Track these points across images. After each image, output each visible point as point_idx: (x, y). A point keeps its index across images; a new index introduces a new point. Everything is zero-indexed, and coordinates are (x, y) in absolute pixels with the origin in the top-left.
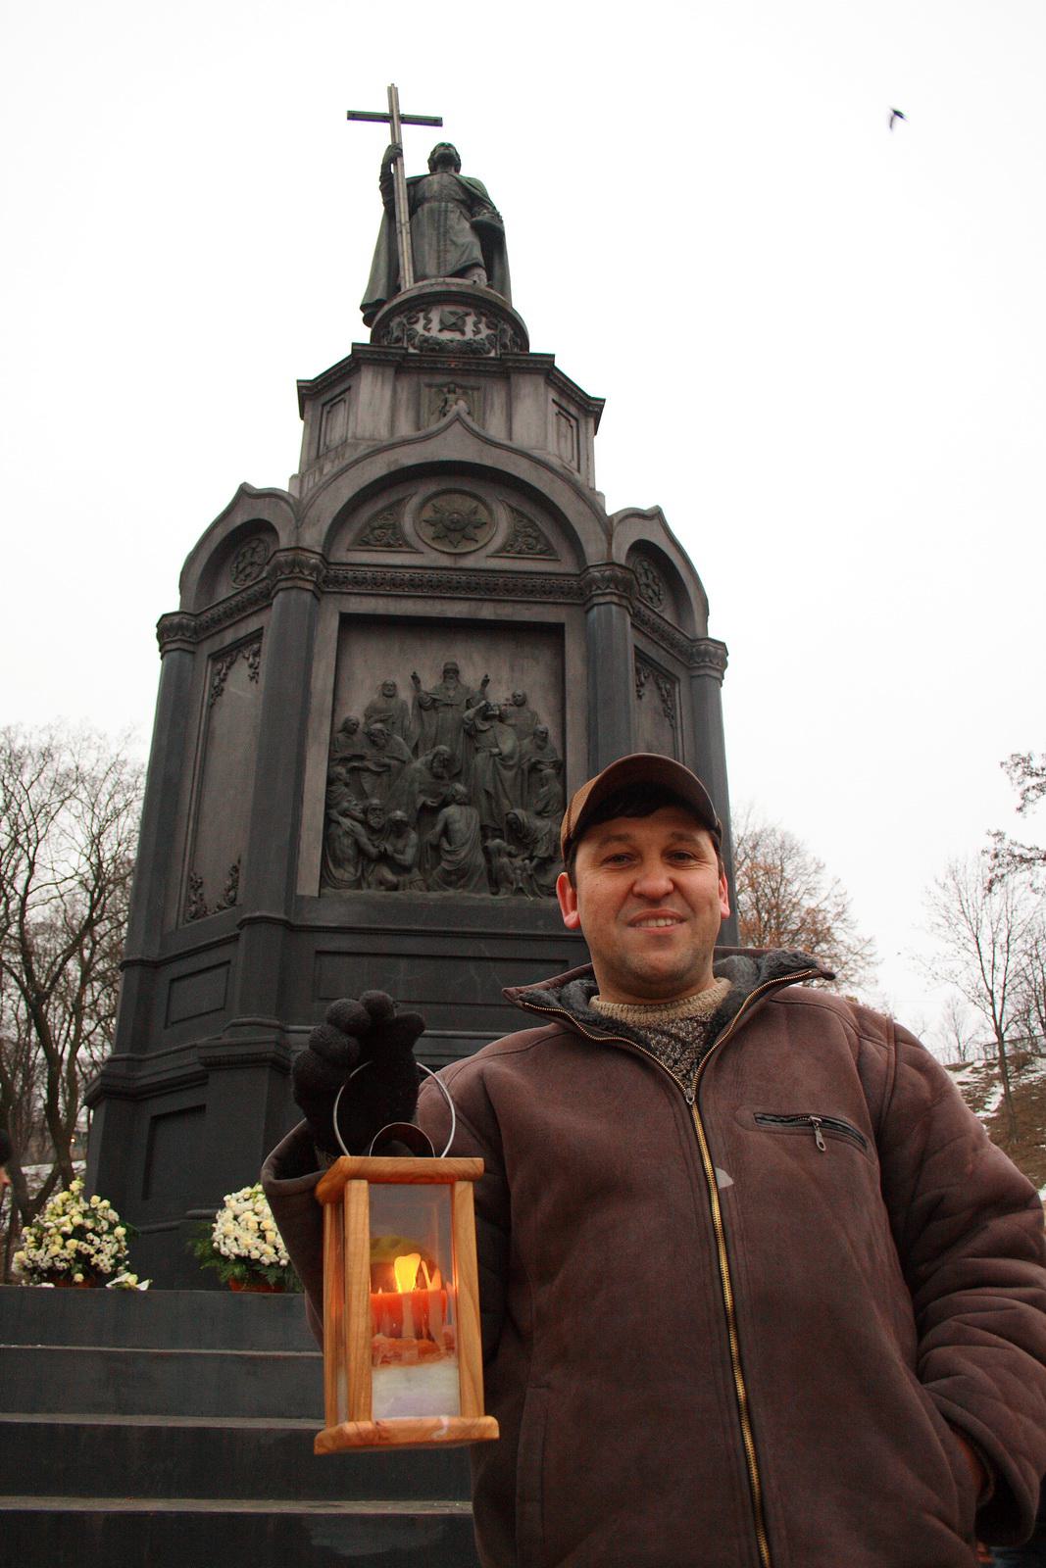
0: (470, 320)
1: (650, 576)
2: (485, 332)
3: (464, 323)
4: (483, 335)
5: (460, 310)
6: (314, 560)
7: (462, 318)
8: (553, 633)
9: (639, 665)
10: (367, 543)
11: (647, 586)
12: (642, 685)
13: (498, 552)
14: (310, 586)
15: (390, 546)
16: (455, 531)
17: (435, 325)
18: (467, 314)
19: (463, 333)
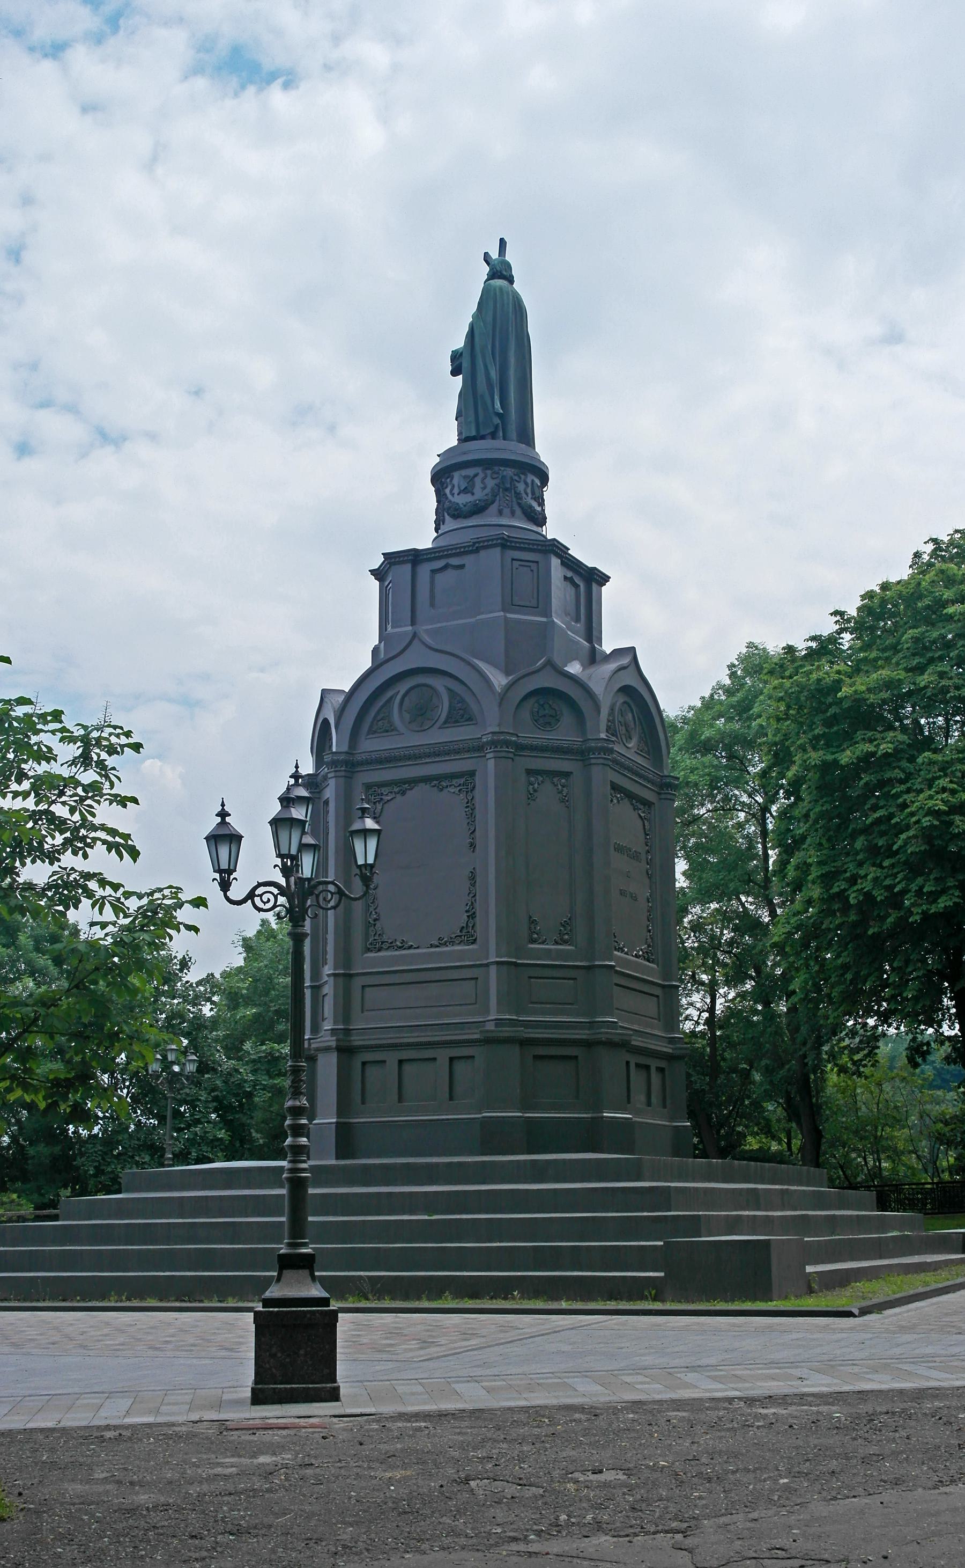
0: (478, 480)
1: (546, 706)
2: (491, 483)
3: (473, 486)
4: (488, 490)
5: (470, 472)
6: (342, 757)
7: (471, 480)
8: (472, 774)
9: (532, 779)
10: (375, 732)
11: (544, 716)
12: (535, 791)
13: (445, 722)
14: (343, 774)
15: (387, 731)
16: (421, 714)
17: (456, 491)
18: (476, 475)
19: (473, 494)
